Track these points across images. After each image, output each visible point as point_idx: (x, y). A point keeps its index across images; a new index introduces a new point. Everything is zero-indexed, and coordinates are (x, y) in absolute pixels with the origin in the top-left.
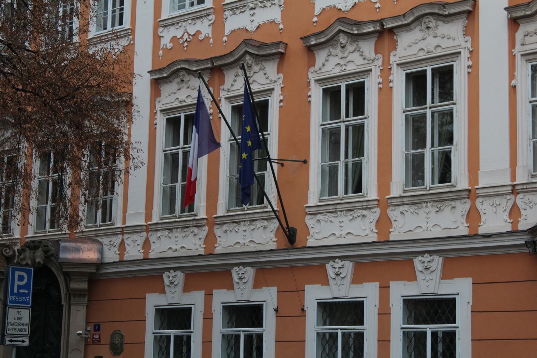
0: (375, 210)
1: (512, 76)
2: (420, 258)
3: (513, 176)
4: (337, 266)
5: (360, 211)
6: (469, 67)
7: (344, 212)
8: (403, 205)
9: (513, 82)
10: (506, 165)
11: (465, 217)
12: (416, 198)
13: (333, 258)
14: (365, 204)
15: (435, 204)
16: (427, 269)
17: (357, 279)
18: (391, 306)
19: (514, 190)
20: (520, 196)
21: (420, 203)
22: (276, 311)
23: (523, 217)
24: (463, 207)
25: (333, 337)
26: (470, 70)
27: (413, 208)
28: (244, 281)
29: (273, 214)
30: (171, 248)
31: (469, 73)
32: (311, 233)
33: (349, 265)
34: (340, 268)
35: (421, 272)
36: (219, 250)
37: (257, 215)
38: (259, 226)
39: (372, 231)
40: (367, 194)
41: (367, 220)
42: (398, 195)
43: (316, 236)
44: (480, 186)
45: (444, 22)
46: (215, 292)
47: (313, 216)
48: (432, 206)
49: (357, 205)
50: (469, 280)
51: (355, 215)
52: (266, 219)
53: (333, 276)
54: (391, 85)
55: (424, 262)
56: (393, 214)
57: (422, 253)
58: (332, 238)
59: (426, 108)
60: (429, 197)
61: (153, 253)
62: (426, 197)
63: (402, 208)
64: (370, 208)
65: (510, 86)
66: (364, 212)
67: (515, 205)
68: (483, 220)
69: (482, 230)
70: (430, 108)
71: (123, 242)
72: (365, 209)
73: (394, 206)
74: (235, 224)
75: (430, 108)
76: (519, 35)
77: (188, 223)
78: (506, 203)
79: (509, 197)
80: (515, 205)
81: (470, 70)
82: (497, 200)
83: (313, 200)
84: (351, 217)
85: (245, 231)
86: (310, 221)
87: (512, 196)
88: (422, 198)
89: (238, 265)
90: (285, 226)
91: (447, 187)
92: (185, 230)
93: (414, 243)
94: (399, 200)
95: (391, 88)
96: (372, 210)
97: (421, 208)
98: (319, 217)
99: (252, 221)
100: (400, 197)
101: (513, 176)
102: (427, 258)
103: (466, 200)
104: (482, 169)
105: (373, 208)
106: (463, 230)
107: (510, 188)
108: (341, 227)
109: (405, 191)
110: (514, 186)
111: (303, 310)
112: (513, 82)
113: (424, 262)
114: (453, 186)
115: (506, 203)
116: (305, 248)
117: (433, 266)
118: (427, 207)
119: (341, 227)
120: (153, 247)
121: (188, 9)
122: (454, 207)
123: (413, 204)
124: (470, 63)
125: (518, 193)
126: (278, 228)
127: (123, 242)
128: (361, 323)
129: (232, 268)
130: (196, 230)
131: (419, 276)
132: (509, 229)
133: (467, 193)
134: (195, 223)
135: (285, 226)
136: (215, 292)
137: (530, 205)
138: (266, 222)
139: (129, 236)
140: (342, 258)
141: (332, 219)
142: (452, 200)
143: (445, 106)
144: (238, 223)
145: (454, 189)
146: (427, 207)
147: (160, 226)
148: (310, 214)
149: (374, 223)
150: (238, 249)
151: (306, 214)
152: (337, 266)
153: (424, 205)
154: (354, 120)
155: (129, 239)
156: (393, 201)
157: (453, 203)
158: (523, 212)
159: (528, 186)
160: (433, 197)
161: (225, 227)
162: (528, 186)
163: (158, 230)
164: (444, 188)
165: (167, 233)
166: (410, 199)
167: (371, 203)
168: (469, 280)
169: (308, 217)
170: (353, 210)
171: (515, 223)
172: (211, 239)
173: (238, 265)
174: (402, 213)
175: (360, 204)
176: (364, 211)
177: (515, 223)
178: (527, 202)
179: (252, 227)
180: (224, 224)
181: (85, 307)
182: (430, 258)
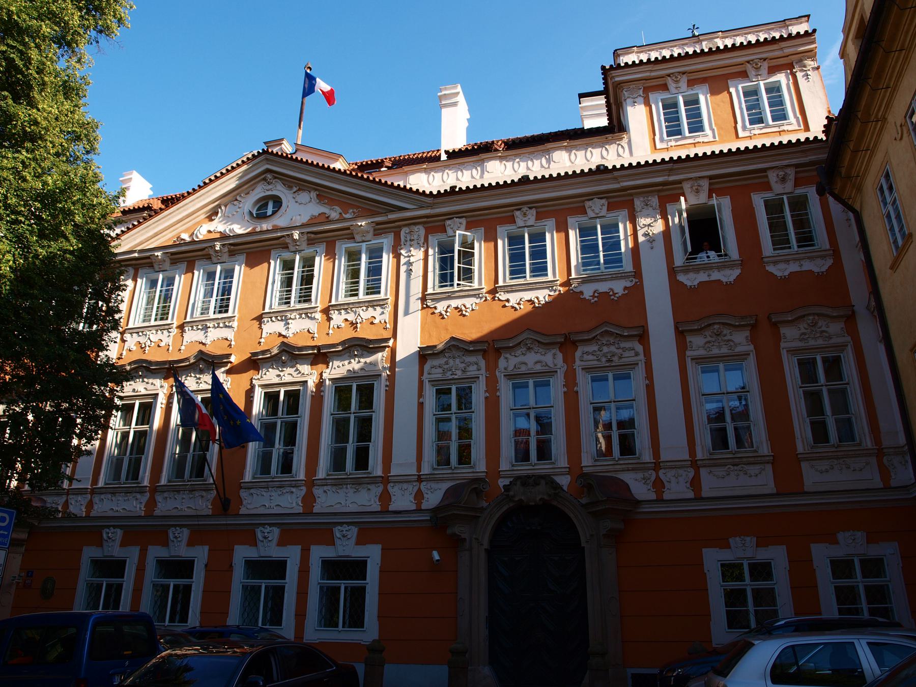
0: (301, 488)
1: (421, 394)
2: (339, 528)
3: (419, 468)
4: (266, 531)
5: (289, 488)
6: (387, 386)
7: (275, 488)
8: (327, 485)
9: (421, 400)
10: (413, 459)
11: (378, 497)
12: (338, 481)
13: (263, 525)
14: (294, 483)
15: (354, 486)
16: (344, 536)
17: (283, 542)
18: (310, 565)
19: (420, 479)
20: (424, 483)
21: (341, 485)
22: (206, 566)
23: (426, 499)
24: (377, 490)
25: (256, 590)
26: (387, 389)
27: (334, 489)
28: (179, 539)
29: (214, 486)
30: (113, 509)
31: (386, 390)
32: (244, 503)
33: (276, 531)
34: (268, 533)
35: (340, 538)
36: (157, 512)
37: (196, 486)
38: (197, 495)
39: (298, 505)
40: (296, 475)
41: (294, 496)
42: (323, 477)
43: (249, 507)
44: (391, 474)
45: (368, 352)
46: (150, 547)
47: (247, 490)
48: (351, 488)
49: (287, 483)
50: (380, 546)
51: (284, 491)
52: (204, 490)
53: (261, 538)
54: (322, 394)
55: (342, 531)
56: (317, 491)
57: (341, 524)
58: (263, 508)
59: (351, 413)
60: (349, 480)
61: (94, 512)
62: (346, 480)
63: (325, 488)
64: (298, 486)
65: (418, 402)
66: (294, 490)
67: (419, 490)
68: (393, 500)
69: (391, 508)
70: (354, 413)
71: (67, 501)
72: (293, 487)
73: (319, 486)
74: (175, 493)
75: (354, 413)
76: (427, 367)
77: (132, 489)
78: (412, 489)
79: (414, 484)
80: (419, 490)
81: (387, 389)
82: (405, 486)
83: (248, 477)
84: (281, 493)
85: (183, 498)
86: (243, 494)
87: (417, 483)
88: (343, 481)
89: (175, 526)
90: (222, 496)
91: (365, 473)
92: (128, 494)
93: (336, 515)
94: (323, 481)
95: (322, 396)
96: (299, 488)
97: (341, 488)
98: (252, 491)
99: (191, 491)
100: (325, 479)
101: (419, 468)
102: (345, 528)
103: (380, 484)
104: (393, 462)
105: (300, 486)
106: (376, 507)
107: (417, 477)
108: (271, 500)
109: (328, 475)
110: (419, 476)
111: (231, 566)
112: (421, 400)
113: (342, 531)
114: (369, 473)
115: (412, 489)
116: (238, 515)
117: (349, 534)
118: (347, 488)
119: (271, 500)
120: (96, 507)
121: (153, 323)
122: (369, 489)
123: (335, 485)
124: (388, 383)
125: (422, 481)
126: (215, 498)
127: (67, 501)
128: (283, 577)
129: (169, 529)
130: (138, 496)
131: (337, 542)
132: (414, 507)
133: (381, 479)
134: (137, 489)
135: (222, 496)
136: (150, 547)
137: (432, 490)
138: (204, 492)
139: (74, 496)
140: (271, 525)
141: (264, 493)
142: (368, 484)
143: (365, 413)
144: (178, 491)
145: (371, 475)
146: (347, 488)
147: (104, 490)
148: (245, 488)
149: (300, 499)
150: (175, 513)
151: (241, 488)
152: (266, 531)
153: (345, 486)
154: (291, 418)
155: (72, 499)
156: (318, 482)
157: (369, 486)
158: (425, 495)
159: (431, 476)
160: (352, 480)
161: (166, 495)
162: (431, 476)
163: (102, 493)
164: (360, 474)
165: (110, 496)
166: (333, 481)
167: (299, 482)
168: (380, 546)
169: (242, 490)
170: (283, 487)
171: (419, 504)
172: (151, 504)
173: (175, 526)
174: (325, 492)
175: (289, 483)
176: (292, 488)
177: (419, 504)
178: (429, 488)
179: (191, 496)
180: (165, 491)
181: (22, 555)
182: (347, 528)
